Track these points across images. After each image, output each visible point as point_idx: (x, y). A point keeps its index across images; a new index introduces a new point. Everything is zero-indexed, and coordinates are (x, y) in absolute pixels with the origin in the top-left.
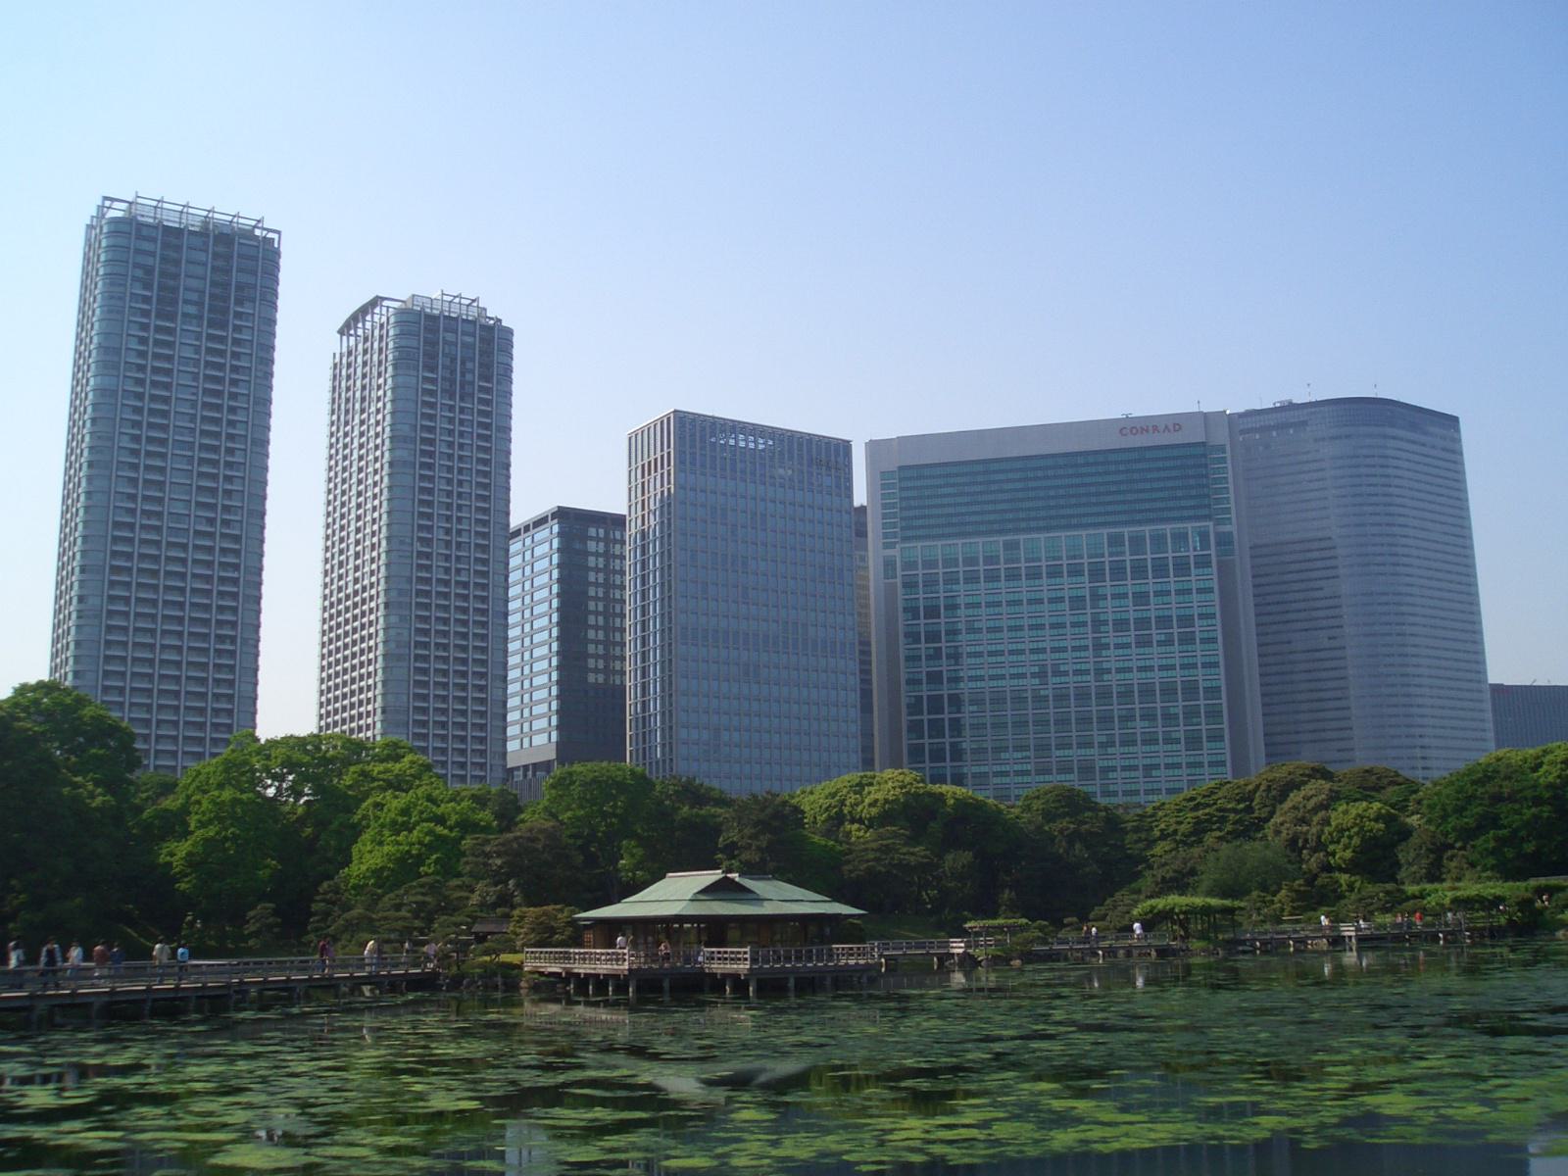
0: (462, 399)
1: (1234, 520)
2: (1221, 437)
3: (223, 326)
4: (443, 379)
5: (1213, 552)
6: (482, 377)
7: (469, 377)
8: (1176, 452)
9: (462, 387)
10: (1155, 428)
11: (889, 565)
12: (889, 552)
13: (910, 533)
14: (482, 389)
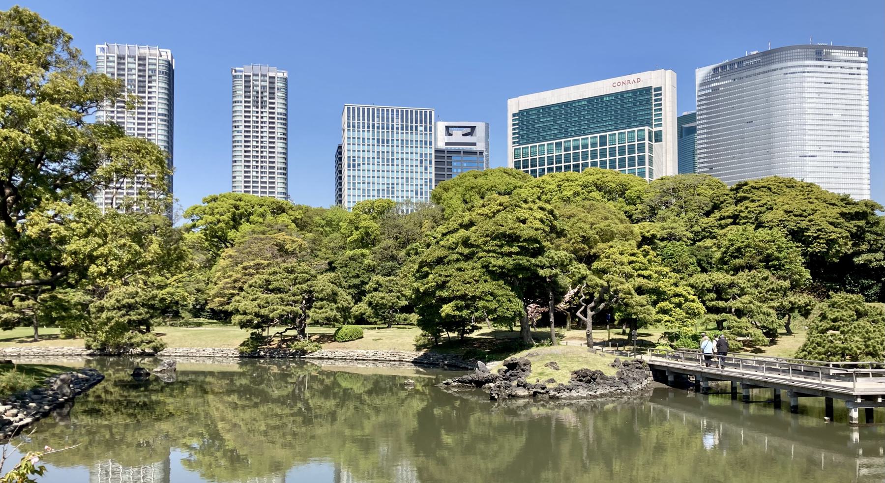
0: (262, 108)
3: (144, 92)
7: (265, 99)
14: (270, 103)
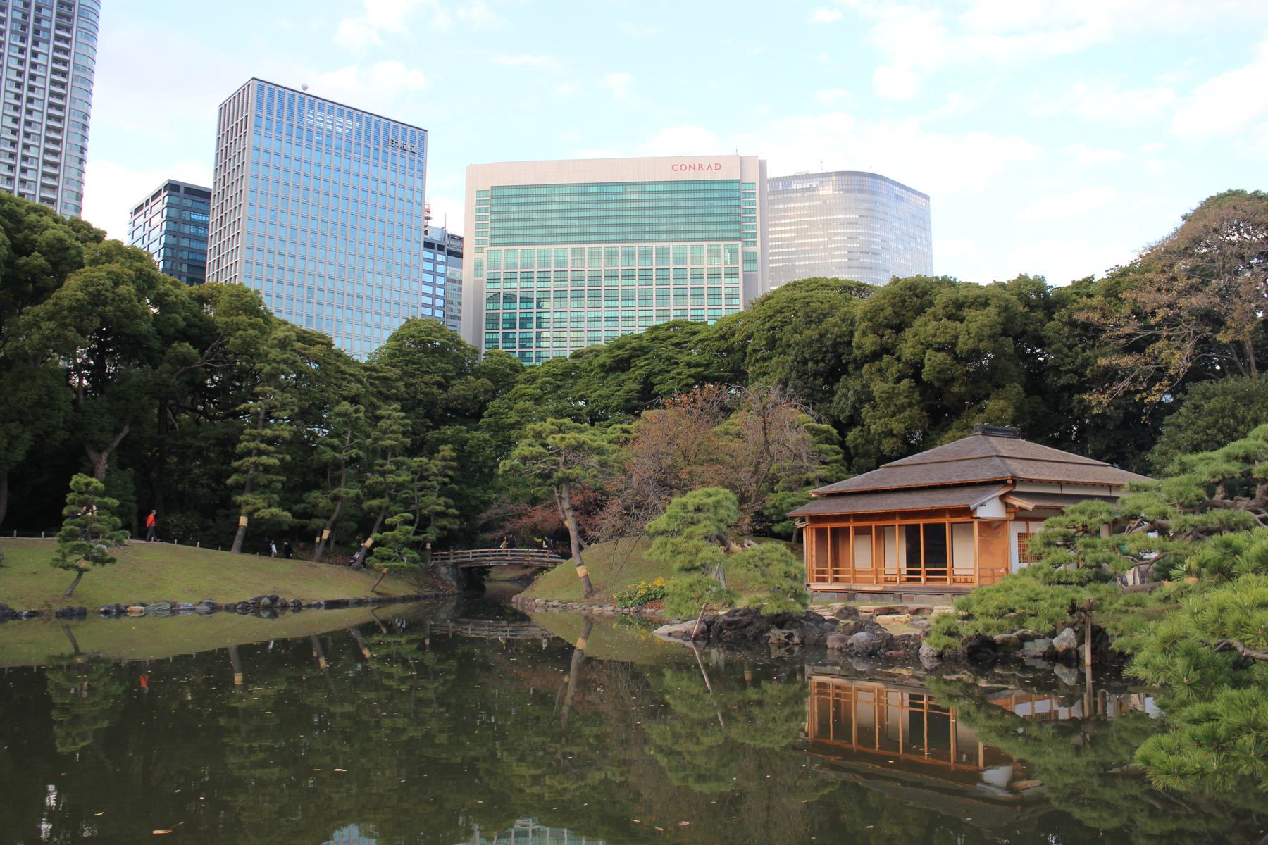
0: (36, 43)
1: (759, 244)
2: (752, 176)
4: (13, 20)
5: (740, 265)
6: (58, 27)
8: (715, 187)
9: (37, 32)
10: (701, 166)
11: (478, 265)
12: (479, 255)
13: (496, 241)
